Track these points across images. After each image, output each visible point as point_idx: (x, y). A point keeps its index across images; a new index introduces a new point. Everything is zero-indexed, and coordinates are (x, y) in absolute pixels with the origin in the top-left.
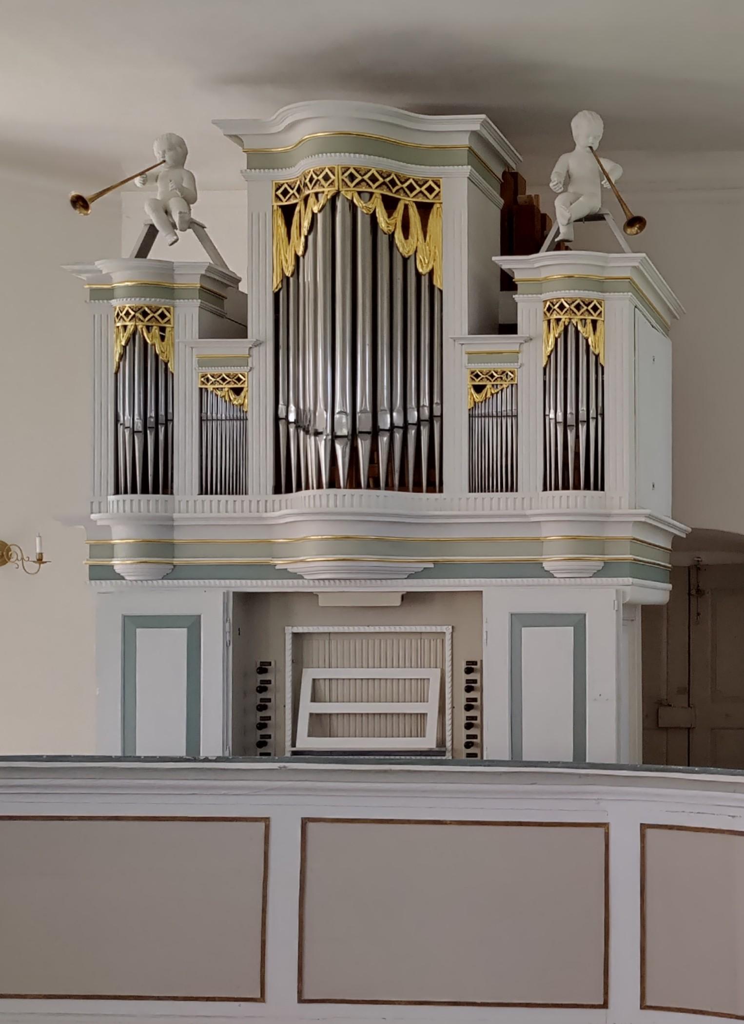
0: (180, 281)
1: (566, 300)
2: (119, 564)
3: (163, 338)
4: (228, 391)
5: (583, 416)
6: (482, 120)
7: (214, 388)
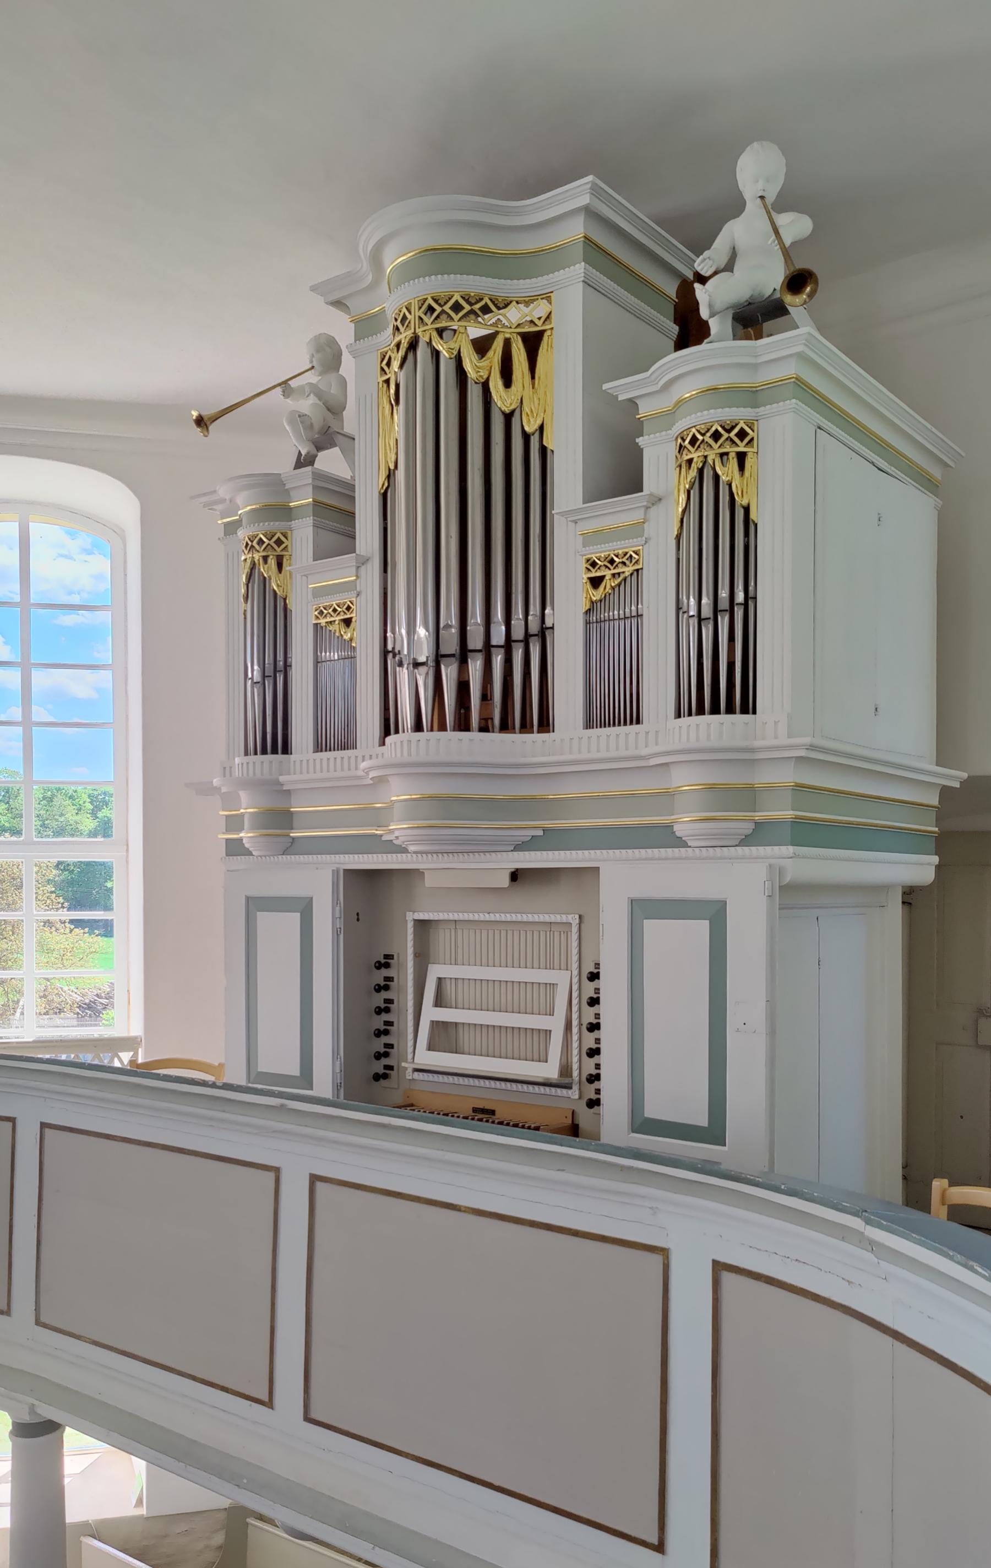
1: (698, 427)
3: (280, 566)
4: (339, 624)
5: (724, 603)
6: (589, 186)
7: (326, 622)
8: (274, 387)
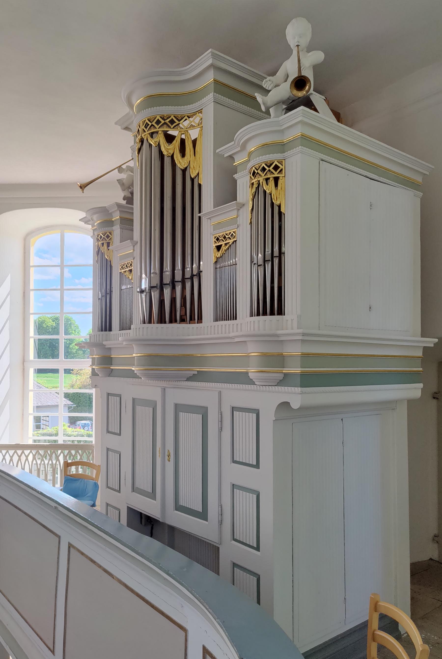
6: (210, 54)
8: (115, 169)
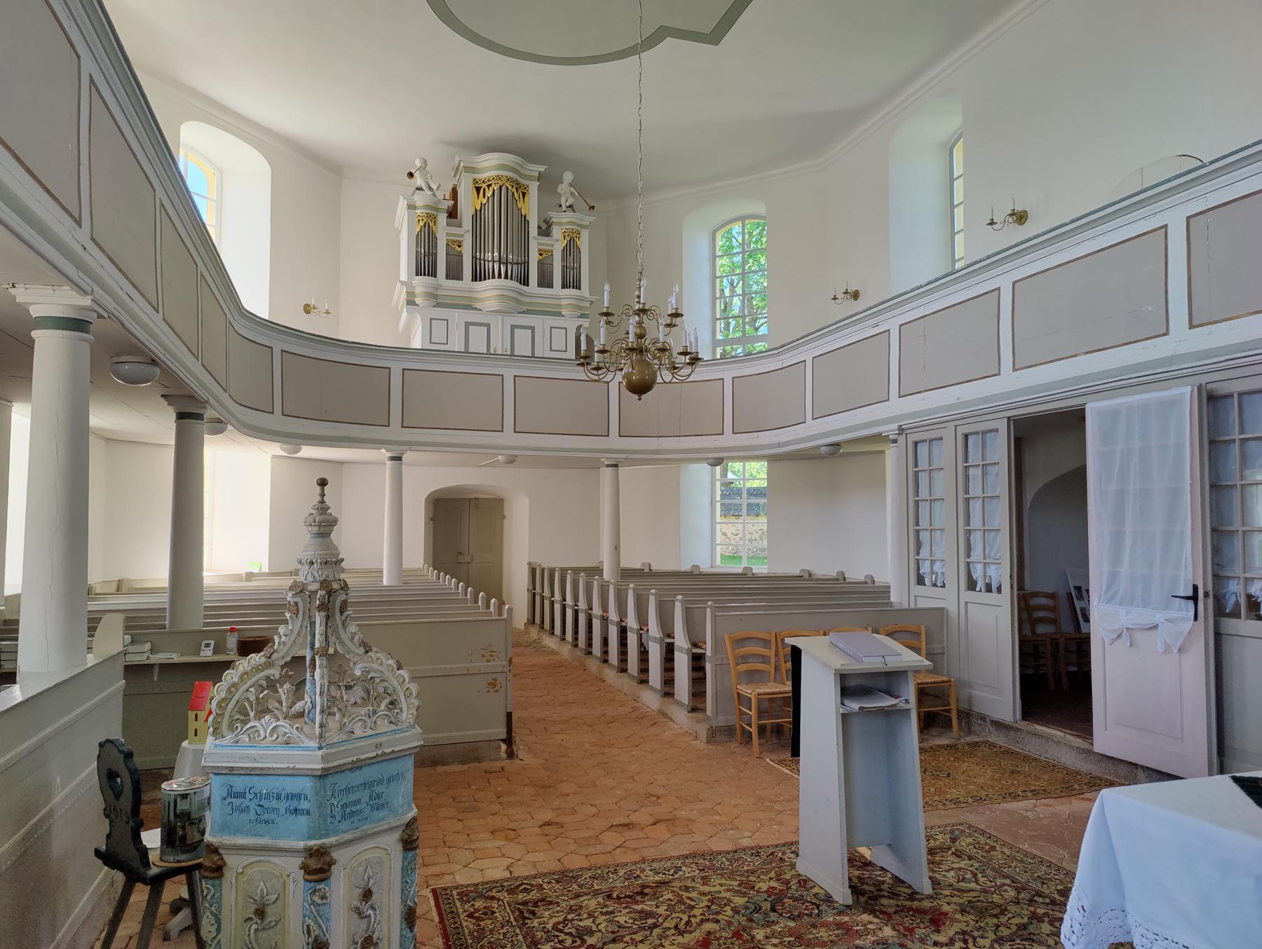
0: (440, 207)
2: (418, 301)
